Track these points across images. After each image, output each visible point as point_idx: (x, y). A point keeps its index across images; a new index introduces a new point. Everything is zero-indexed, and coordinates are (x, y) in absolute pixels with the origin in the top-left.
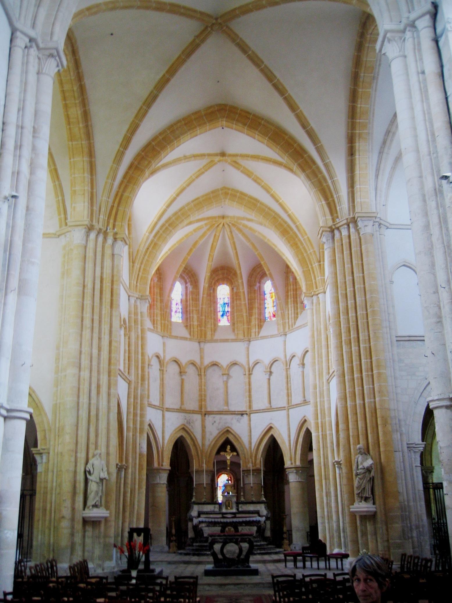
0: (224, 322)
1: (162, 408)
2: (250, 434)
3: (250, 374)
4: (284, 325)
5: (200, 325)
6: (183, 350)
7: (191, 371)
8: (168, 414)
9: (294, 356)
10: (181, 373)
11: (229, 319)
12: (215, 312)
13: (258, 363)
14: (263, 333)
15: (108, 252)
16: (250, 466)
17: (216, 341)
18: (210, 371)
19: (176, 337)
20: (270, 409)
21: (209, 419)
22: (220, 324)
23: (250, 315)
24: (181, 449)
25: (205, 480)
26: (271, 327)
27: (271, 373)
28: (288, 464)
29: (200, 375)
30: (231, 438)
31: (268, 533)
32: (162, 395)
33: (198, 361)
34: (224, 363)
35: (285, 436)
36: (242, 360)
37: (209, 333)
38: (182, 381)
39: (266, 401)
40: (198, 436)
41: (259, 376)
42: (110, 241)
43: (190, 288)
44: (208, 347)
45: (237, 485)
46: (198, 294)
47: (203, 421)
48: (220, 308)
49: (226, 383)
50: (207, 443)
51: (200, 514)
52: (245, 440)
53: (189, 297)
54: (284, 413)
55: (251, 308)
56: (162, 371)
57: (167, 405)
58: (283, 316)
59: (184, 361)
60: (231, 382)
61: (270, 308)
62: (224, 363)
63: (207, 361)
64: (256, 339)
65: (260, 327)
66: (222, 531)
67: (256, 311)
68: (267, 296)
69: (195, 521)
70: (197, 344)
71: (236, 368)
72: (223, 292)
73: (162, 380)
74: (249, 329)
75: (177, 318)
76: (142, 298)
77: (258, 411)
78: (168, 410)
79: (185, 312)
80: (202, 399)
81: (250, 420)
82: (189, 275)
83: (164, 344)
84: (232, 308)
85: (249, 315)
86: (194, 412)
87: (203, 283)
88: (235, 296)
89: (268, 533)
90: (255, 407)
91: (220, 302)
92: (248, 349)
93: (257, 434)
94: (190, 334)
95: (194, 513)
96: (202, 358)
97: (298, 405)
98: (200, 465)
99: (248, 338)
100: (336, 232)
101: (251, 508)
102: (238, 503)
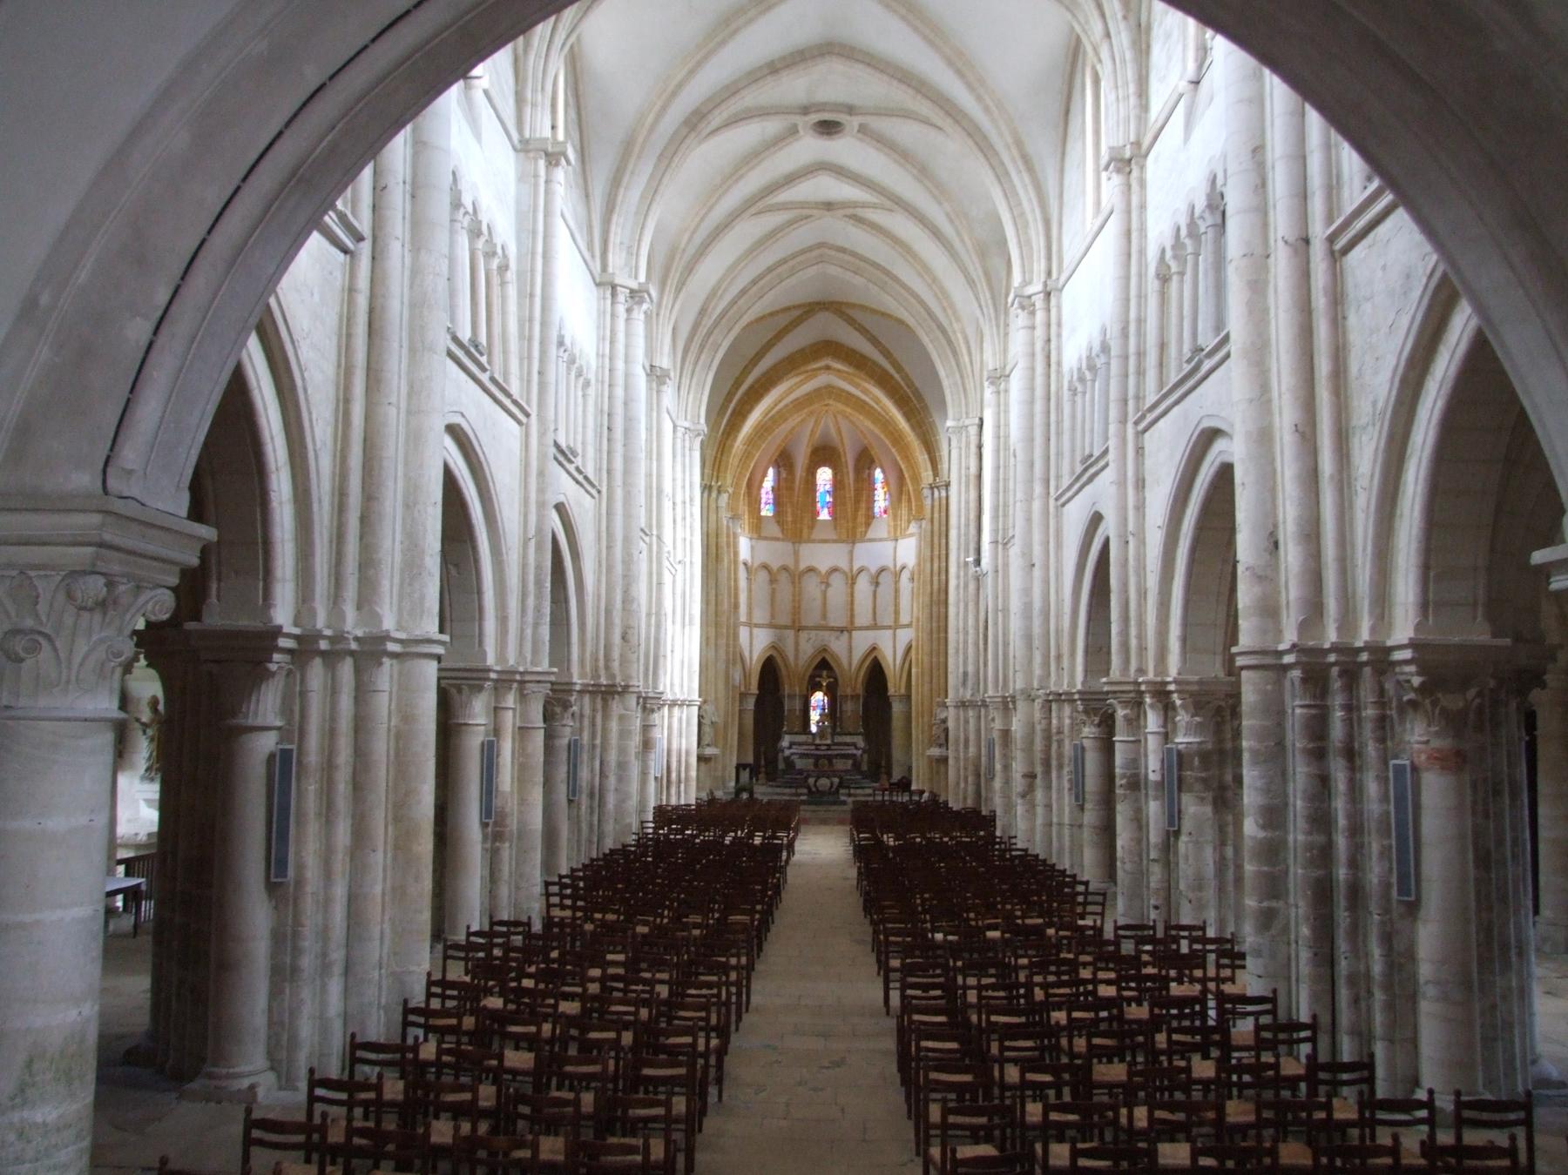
0: (824, 515)
1: (751, 625)
2: (850, 653)
3: (853, 583)
4: (895, 527)
5: (794, 522)
6: (776, 553)
7: (783, 577)
8: (756, 631)
10: (773, 581)
12: (814, 503)
14: (870, 535)
15: (713, 506)
16: (849, 691)
17: (814, 541)
18: (806, 577)
19: (766, 538)
20: (875, 627)
21: (804, 635)
23: (856, 510)
24: (770, 670)
25: (798, 705)
26: (881, 528)
27: (877, 584)
28: (891, 691)
30: (828, 658)
31: (865, 767)
33: (790, 563)
34: (823, 568)
35: (890, 659)
36: (844, 565)
37: (805, 531)
38: (773, 592)
39: (870, 615)
41: (863, 585)
42: (714, 495)
43: (784, 475)
45: (833, 713)
46: (793, 481)
47: (797, 637)
49: (824, 593)
50: (801, 662)
51: (791, 745)
52: (845, 662)
53: (783, 484)
54: (889, 633)
55: (857, 501)
57: (755, 621)
58: (895, 517)
59: (775, 566)
60: (830, 591)
61: (881, 500)
62: (823, 568)
63: (802, 566)
64: (863, 541)
65: (868, 525)
66: (816, 765)
67: (863, 505)
68: (879, 485)
69: (787, 753)
70: (788, 546)
71: (836, 574)
72: (824, 476)
74: (854, 528)
75: (767, 511)
77: (860, 629)
79: (778, 503)
80: (796, 611)
82: (784, 461)
84: (835, 498)
85: (853, 513)
86: (786, 627)
88: (838, 484)
89: (865, 767)
92: (851, 552)
93: (858, 654)
95: (785, 743)
96: (797, 562)
98: (790, 688)
101: (848, 739)
102: (834, 734)
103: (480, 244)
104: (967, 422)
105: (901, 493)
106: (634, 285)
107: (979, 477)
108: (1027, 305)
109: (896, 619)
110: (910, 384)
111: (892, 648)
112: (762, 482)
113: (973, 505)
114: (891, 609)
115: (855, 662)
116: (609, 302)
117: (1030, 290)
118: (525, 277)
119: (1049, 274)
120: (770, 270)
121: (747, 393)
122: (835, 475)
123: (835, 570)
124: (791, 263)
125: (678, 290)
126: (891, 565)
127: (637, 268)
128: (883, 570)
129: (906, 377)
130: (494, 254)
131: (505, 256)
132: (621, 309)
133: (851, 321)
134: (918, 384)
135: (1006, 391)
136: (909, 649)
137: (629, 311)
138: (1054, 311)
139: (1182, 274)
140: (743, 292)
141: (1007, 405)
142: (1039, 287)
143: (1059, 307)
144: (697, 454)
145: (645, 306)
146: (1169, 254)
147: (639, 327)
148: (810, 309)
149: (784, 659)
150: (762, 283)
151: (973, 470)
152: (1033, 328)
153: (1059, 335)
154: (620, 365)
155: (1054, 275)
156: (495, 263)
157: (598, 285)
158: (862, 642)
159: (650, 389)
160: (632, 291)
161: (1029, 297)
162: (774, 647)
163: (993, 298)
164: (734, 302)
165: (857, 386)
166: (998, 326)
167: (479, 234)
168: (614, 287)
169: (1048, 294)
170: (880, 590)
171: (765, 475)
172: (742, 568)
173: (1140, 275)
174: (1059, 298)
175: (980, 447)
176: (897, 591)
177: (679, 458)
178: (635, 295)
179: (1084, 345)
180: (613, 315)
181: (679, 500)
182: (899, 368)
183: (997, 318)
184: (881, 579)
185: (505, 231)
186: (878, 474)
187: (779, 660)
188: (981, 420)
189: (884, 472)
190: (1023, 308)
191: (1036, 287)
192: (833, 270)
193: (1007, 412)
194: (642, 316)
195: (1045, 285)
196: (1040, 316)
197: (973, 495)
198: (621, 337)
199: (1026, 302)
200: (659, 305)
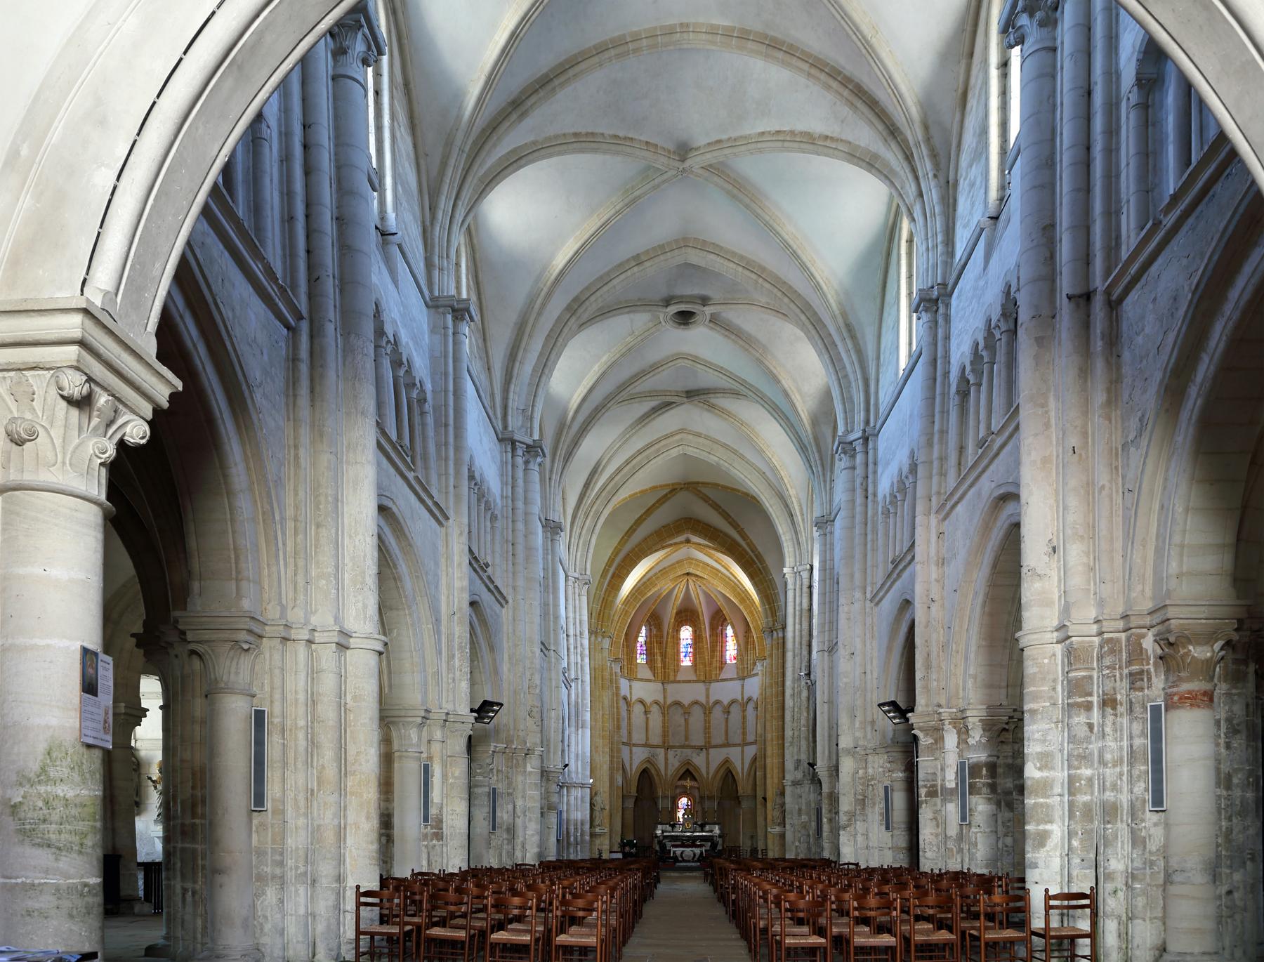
0: (687, 662)
1: (629, 744)
5: (664, 667)
7: (655, 709)
8: (634, 749)
12: (678, 652)
17: (679, 682)
19: (641, 680)
20: (727, 745)
21: (671, 753)
22: (683, 664)
23: (712, 657)
28: (740, 792)
29: (663, 713)
30: (691, 769)
32: (630, 733)
36: (703, 699)
40: (662, 767)
41: (717, 713)
43: (654, 631)
44: (669, 687)
47: (666, 754)
48: (683, 650)
50: (669, 773)
55: (713, 650)
56: (629, 711)
58: (742, 661)
59: (648, 700)
60: (691, 720)
61: (731, 649)
62: (686, 702)
63: (669, 701)
64: (717, 681)
65: (721, 668)
72: (686, 633)
73: (629, 719)
75: (641, 659)
76: (616, 660)
78: (635, 745)
80: (665, 735)
81: (708, 754)
82: (654, 621)
84: (695, 649)
86: (658, 746)
88: (697, 638)
90: (714, 742)
91: (683, 643)
92: (707, 690)
93: (714, 766)
97: (751, 744)
99: (707, 680)
103: (401, 373)
104: (800, 568)
105: (747, 643)
106: (529, 442)
107: (810, 610)
108: (848, 448)
109: (744, 739)
110: (754, 550)
111: (740, 759)
112: (637, 637)
113: (805, 633)
114: (739, 731)
115: (712, 772)
116: (510, 455)
117: (852, 437)
118: (440, 410)
119: (867, 422)
120: (640, 452)
121: (624, 560)
122: (695, 632)
123: (696, 703)
124: (657, 446)
125: (567, 460)
126: (739, 698)
127: (531, 428)
128: (733, 702)
129: (750, 544)
130: (414, 385)
131: (422, 391)
132: (520, 461)
133: (706, 499)
134: (760, 549)
135: (831, 533)
136: (755, 759)
137: (527, 463)
138: (871, 453)
139: (979, 385)
140: (619, 470)
141: (832, 544)
142: (859, 434)
143: (875, 449)
144: (584, 599)
145: (539, 460)
146: (968, 369)
147: (535, 477)
148: (673, 490)
149: (658, 771)
150: (634, 462)
151: (805, 605)
152: (854, 468)
153: (875, 472)
154: (520, 504)
155: (872, 424)
156: (414, 394)
157: (500, 440)
158: (717, 756)
159: (545, 538)
160: (528, 446)
161: (851, 443)
162: (648, 761)
163: (821, 459)
164: (611, 479)
166: (825, 481)
167: (401, 364)
168: (513, 442)
169: (866, 439)
170: (732, 717)
171: (639, 631)
172: (622, 703)
173: (943, 394)
174: (875, 442)
175: (810, 587)
176: (744, 717)
177: (570, 601)
178: (533, 449)
179: (896, 472)
180: (513, 466)
181: (571, 632)
182: (744, 537)
183: (824, 475)
184: (732, 709)
185: (421, 367)
186: (729, 631)
187: (653, 771)
188: (812, 567)
189: (733, 628)
190: (845, 452)
191: (857, 434)
192: (690, 451)
193: (832, 549)
194: (537, 468)
195: (864, 431)
196: (859, 458)
197: (805, 625)
198: (520, 482)
199: (848, 447)
200: (551, 471)
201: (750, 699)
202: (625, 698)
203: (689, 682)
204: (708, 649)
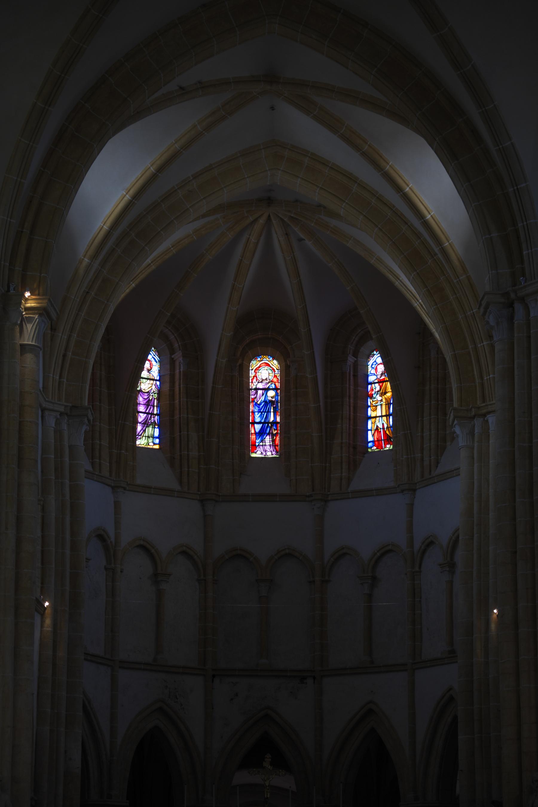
9: (431, 543)
10: (158, 577)
11: (278, 441)
13: (345, 554)
19: (146, 489)
72: (264, 373)
83: (117, 505)
87: (214, 357)
94: (181, 483)
100: (518, 306)
128: (386, 551)
165: (332, 124)
186: (376, 366)
201: (429, 543)
202: (101, 537)
203: (270, 498)
204: (323, 403)
